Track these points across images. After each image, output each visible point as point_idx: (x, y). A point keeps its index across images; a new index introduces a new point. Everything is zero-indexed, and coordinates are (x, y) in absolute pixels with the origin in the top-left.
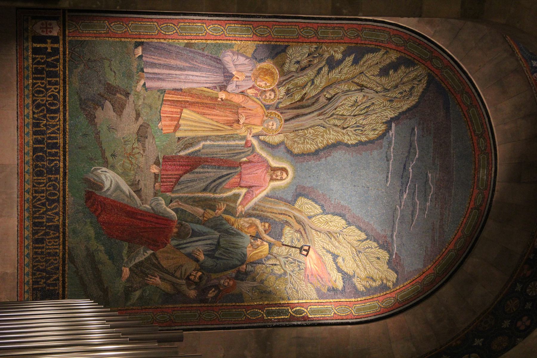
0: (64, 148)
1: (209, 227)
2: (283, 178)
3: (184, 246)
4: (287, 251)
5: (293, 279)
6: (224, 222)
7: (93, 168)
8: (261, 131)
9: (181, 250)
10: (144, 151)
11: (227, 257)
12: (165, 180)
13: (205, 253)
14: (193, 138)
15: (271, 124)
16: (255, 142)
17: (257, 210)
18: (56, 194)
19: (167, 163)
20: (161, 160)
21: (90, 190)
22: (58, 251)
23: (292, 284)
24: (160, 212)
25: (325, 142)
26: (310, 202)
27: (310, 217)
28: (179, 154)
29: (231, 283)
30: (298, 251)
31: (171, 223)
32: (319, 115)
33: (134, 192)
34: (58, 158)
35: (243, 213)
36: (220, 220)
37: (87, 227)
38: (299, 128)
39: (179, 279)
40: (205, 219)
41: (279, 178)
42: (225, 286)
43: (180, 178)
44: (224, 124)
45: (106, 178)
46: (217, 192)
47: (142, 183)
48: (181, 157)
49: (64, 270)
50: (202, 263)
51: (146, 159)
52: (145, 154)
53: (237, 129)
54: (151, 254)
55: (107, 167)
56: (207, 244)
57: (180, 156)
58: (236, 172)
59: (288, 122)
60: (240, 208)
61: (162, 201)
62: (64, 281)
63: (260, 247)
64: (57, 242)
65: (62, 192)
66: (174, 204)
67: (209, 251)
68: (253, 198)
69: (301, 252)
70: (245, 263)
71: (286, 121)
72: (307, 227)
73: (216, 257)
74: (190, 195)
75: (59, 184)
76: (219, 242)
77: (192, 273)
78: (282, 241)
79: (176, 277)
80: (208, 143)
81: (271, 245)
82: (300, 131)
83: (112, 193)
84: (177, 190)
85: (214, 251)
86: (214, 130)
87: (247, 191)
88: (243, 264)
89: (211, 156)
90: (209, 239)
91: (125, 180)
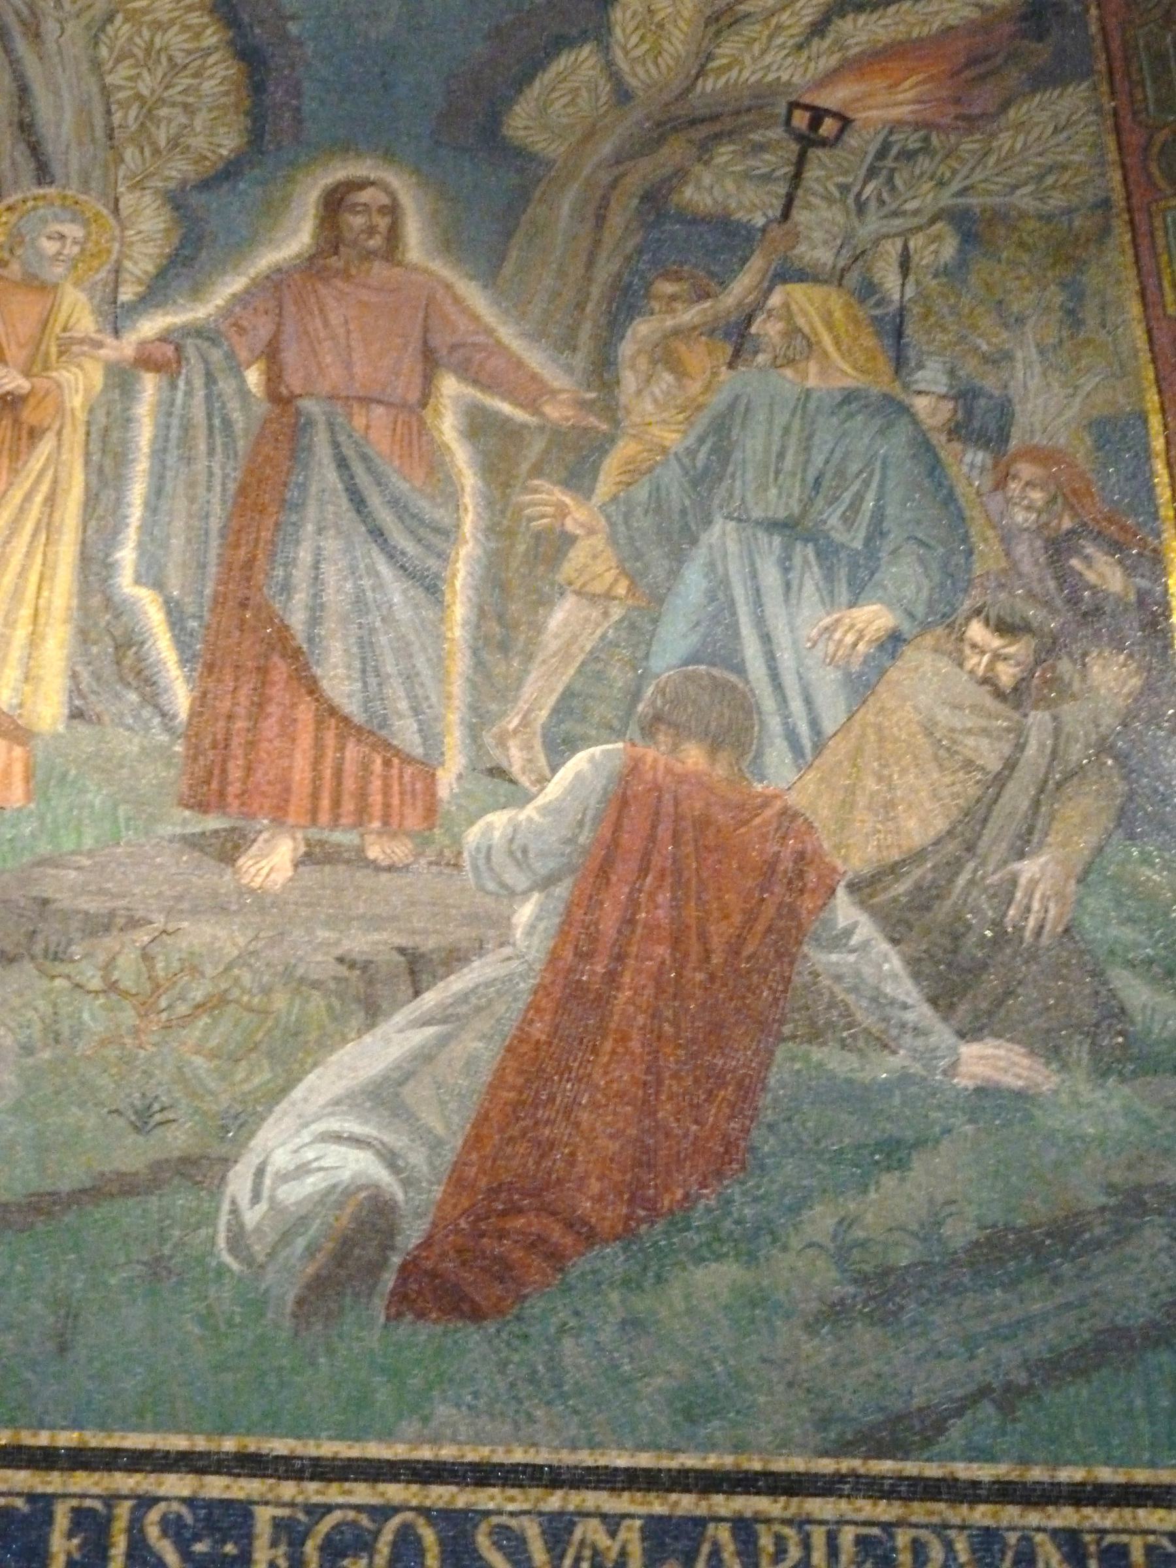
0: (45, 1459)
1: (674, 574)
2: (385, 200)
3: (796, 705)
4: (815, 201)
5: (985, 181)
6: (642, 493)
7: (227, 1259)
8: (91, 292)
9: (829, 727)
10: (134, 923)
11: (867, 484)
12: (348, 805)
13: (844, 596)
14: (84, 636)
15: (50, 247)
16: (150, 326)
17: (574, 330)
18: (406, 1536)
19: (233, 789)
20: (213, 822)
21: (389, 1279)
22: (847, 1536)
23: (1015, 187)
24: (571, 841)
25: (194, 18)
26: (536, 88)
27: (623, 95)
28: (183, 714)
29: (1026, 470)
30: (815, 153)
31: (649, 776)
32: (36, 36)
33: (417, 993)
34: (123, 1510)
35: (592, 395)
36: (627, 516)
37: (664, 1313)
38: (99, 121)
39: (1020, 747)
40: (621, 590)
41: (383, 223)
42: (1053, 500)
43: (346, 720)
44: (14, 472)
45: (303, 1170)
46: (447, 521)
47: (359, 943)
48: (202, 701)
49: (1004, 1492)
50: (911, 615)
51: (195, 912)
52: (159, 921)
53: (60, 409)
54: (862, 904)
55: (227, 1162)
56: (788, 586)
57: (193, 714)
58: (331, 426)
59: (57, 169)
60: (553, 412)
61: (490, 827)
62: (1078, 1495)
63: (801, 321)
64: (780, 1540)
65: (395, 1492)
66: (515, 758)
67: (830, 577)
68: (498, 342)
69: (823, 143)
70: (902, 396)
71: (43, 173)
72: (679, 110)
73: (868, 540)
74: (460, 665)
75: (329, 1509)
76: (773, 526)
77: (981, 671)
78: (760, 221)
79: (1011, 765)
80: (127, 555)
81: (787, 274)
82: (117, 118)
83: (420, 1132)
84: (425, 739)
85: (827, 553)
86: (48, 527)
87: (455, 372)
88: (905, 410)
89: (215, 543)
90: (754, 575)
91: (327, 1043)
